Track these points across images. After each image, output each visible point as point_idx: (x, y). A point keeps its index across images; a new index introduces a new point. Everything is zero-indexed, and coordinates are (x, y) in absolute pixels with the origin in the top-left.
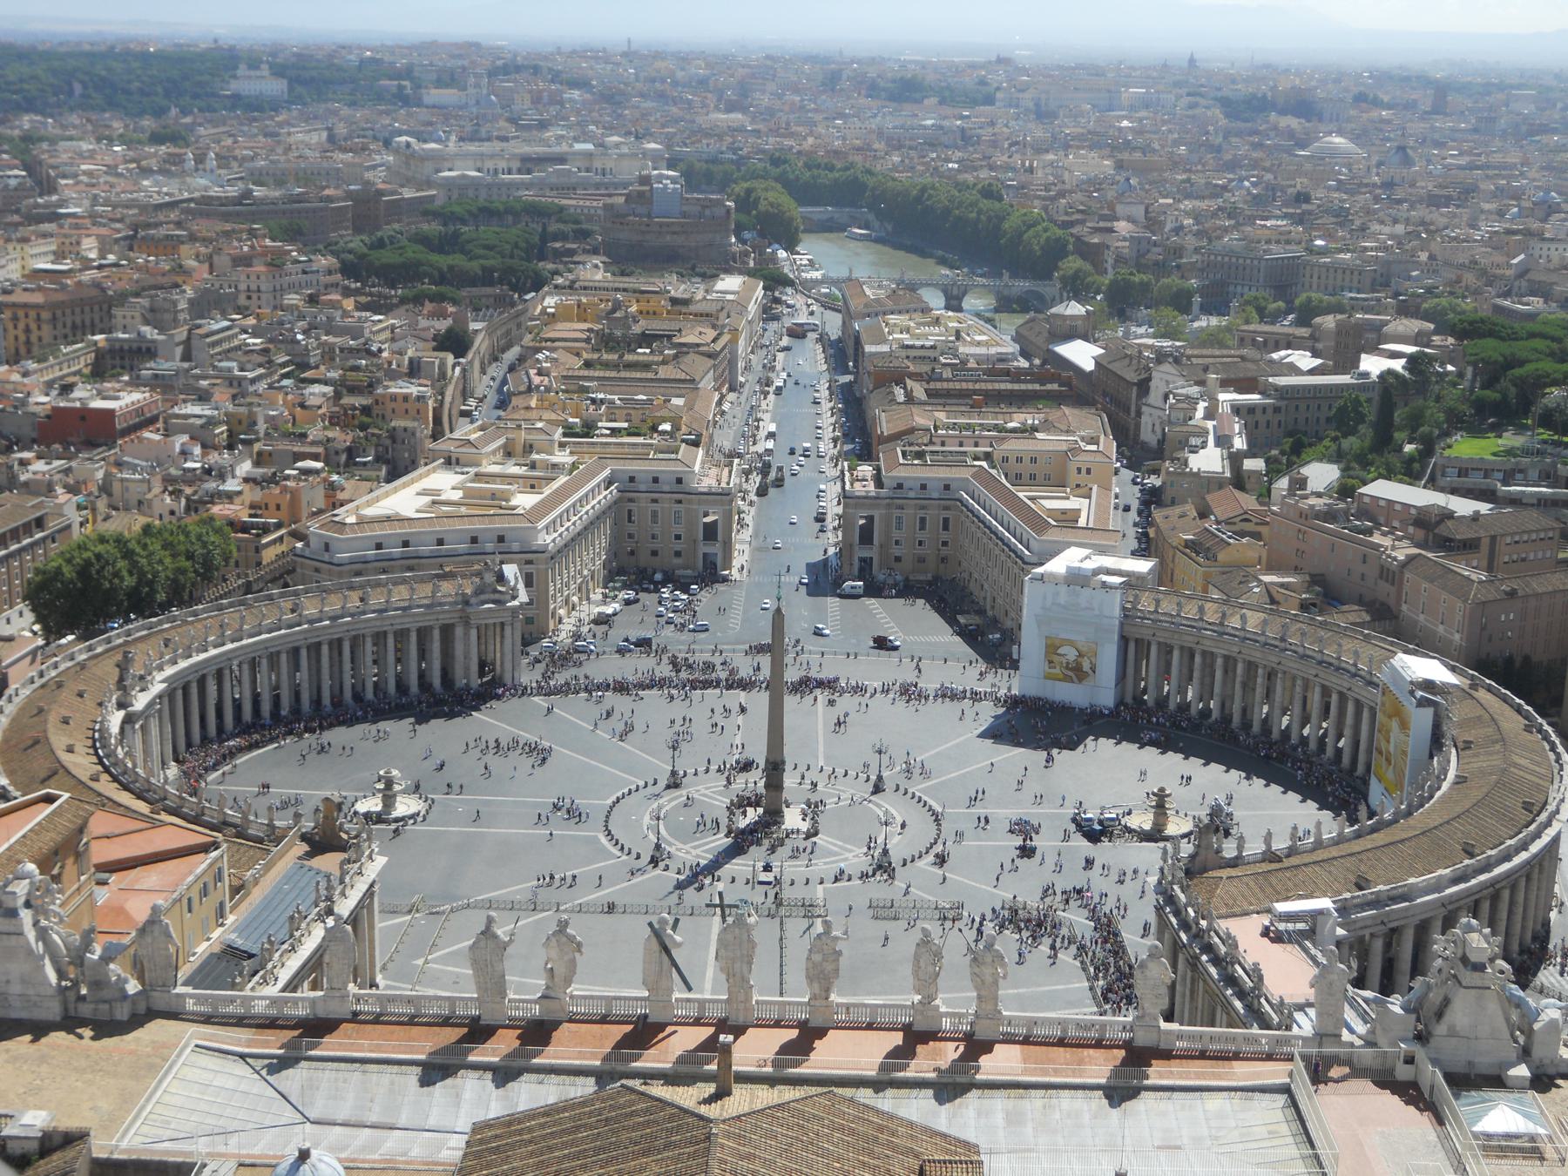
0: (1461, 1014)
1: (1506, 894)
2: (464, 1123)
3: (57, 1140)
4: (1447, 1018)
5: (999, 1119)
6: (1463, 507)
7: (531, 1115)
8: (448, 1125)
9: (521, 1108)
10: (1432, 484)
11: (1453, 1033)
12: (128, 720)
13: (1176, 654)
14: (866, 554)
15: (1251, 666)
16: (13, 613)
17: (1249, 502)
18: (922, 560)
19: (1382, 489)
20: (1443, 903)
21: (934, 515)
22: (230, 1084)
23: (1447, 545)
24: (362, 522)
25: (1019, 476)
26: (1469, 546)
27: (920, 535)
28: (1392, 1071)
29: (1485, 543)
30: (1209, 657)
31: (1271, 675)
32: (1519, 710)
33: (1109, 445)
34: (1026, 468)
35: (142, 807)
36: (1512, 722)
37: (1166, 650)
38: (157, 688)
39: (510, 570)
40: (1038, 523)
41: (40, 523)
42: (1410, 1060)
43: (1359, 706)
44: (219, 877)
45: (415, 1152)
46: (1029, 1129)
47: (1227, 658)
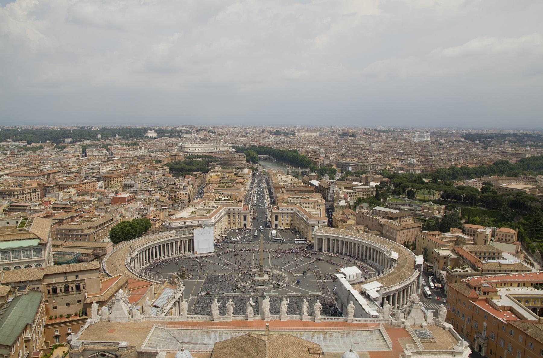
0: (412, 314)
2: (212, 342)
3: (129, 348)
4: (411, 314)
5: (322, 339)
7: (227, 341)
9: (223, 340)
10: (387, 207)
11: (411, 317)
12: (132, 258)
14: (276, 223)
15: (354, 243)
16: (107, 238)
17: (352, 211)
18: (287, 224)
19: (377, 208)
20: (397, 290)
22: (163, 336)
23: (391, 219)
24: (177, 219)
26: (396, 218)
27: (288, 219)
28: (399, 326)
29: (399, 219)
30: (347, 242)
33: (323, 201)
35: (136, 277)
38: (137, 253)
40: (311, 216)
41: (112, 220)
42: (403, 323)
43: (377, 251)
45: (203, 349)
46: (328, 341)
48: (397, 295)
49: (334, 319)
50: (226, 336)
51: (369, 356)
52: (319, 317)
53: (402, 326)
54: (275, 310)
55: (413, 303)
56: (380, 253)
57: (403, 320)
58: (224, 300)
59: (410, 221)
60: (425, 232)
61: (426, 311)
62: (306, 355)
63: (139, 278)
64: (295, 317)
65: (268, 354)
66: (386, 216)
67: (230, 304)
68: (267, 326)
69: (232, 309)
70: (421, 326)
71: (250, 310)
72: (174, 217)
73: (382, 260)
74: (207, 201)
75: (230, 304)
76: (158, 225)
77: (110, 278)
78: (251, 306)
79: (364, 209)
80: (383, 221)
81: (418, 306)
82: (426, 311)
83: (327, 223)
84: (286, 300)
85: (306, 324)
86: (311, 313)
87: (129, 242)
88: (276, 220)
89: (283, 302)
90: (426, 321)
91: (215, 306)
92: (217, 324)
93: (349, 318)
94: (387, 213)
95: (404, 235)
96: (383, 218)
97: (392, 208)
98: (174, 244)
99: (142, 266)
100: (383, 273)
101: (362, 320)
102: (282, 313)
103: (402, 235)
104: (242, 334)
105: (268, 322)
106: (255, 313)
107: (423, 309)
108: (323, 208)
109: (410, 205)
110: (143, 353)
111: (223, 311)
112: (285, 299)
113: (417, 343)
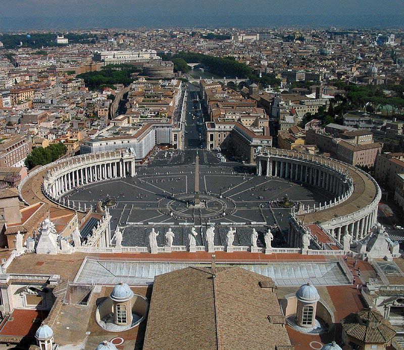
0: (377, 244)
1: (368, 217)
6: (351, 129)
8: (147, 276)
11: (375, 249)
13: (287, 164)
15: (304, 166)
17: (300, 129)
19: (331, 125)
21: (228, 133)
23: (347, 138)
25: (246, 124)
26: (353, 138)
29: (356, 137)
31: (308, 169)
32: (367, 175)
34: (248, 122)
36: (365, 179)
37: (285, 164)
39: (132, 149)
44: (76, 221)
47: (299, 165)
48: (353, 225)
49: (286, 250)
50: (166, 269)
51: (326, 291)
52: (270, 250)
53: (364, 258)
54: (220, 239)
55: (378, 233)
56: (333, 177)
57: (366, 252)
58: (164, 230)
59: (367, 139)
60: (387, 153)
61: (392, 243)
62: (257, 289)
63: (59, 206)
64: (243, 249)
65: (216, 288)
66: (339, 133)
67: (170, 235)
68: (213, 258)
69: (172, 241)
70: (385, 259)
71: (193, 241)
72: (93, 137)
73: (336, 186)
74: (131, 118)
75: (170, 235)
76: (76, 146)
77: (27, 208)
78: (193, 235)
79: (314, 126)
80: (338, 141)
81: (383, 237)
82: (392, 243)
83: (271, 143)
84: (233, 229)
85: (255, 256)
86: (261, 242)
87: (44, 167)
88: (212, 139)
89: (230, 232)
90: (391, 253)
91: (153, 236)
92: (155, 256)
93: (303, 249)
94: (342, 132)
95: (362, 157)
96: (338, 137)
97: (348, 125)
98: (96, 167)
99: (60, 193)
100: (337, 200)
101: (318, 252)
102: (229, 244)
103: (360, 156)
104: (183, 267)
105: (214, 254)
106: (197, 245)
107: (389, 240)
108: (266, 124)
109: (369, 122)
110: (76, 287)
111: (162, 241)
112: (231, 229)
113: (381, 277)
